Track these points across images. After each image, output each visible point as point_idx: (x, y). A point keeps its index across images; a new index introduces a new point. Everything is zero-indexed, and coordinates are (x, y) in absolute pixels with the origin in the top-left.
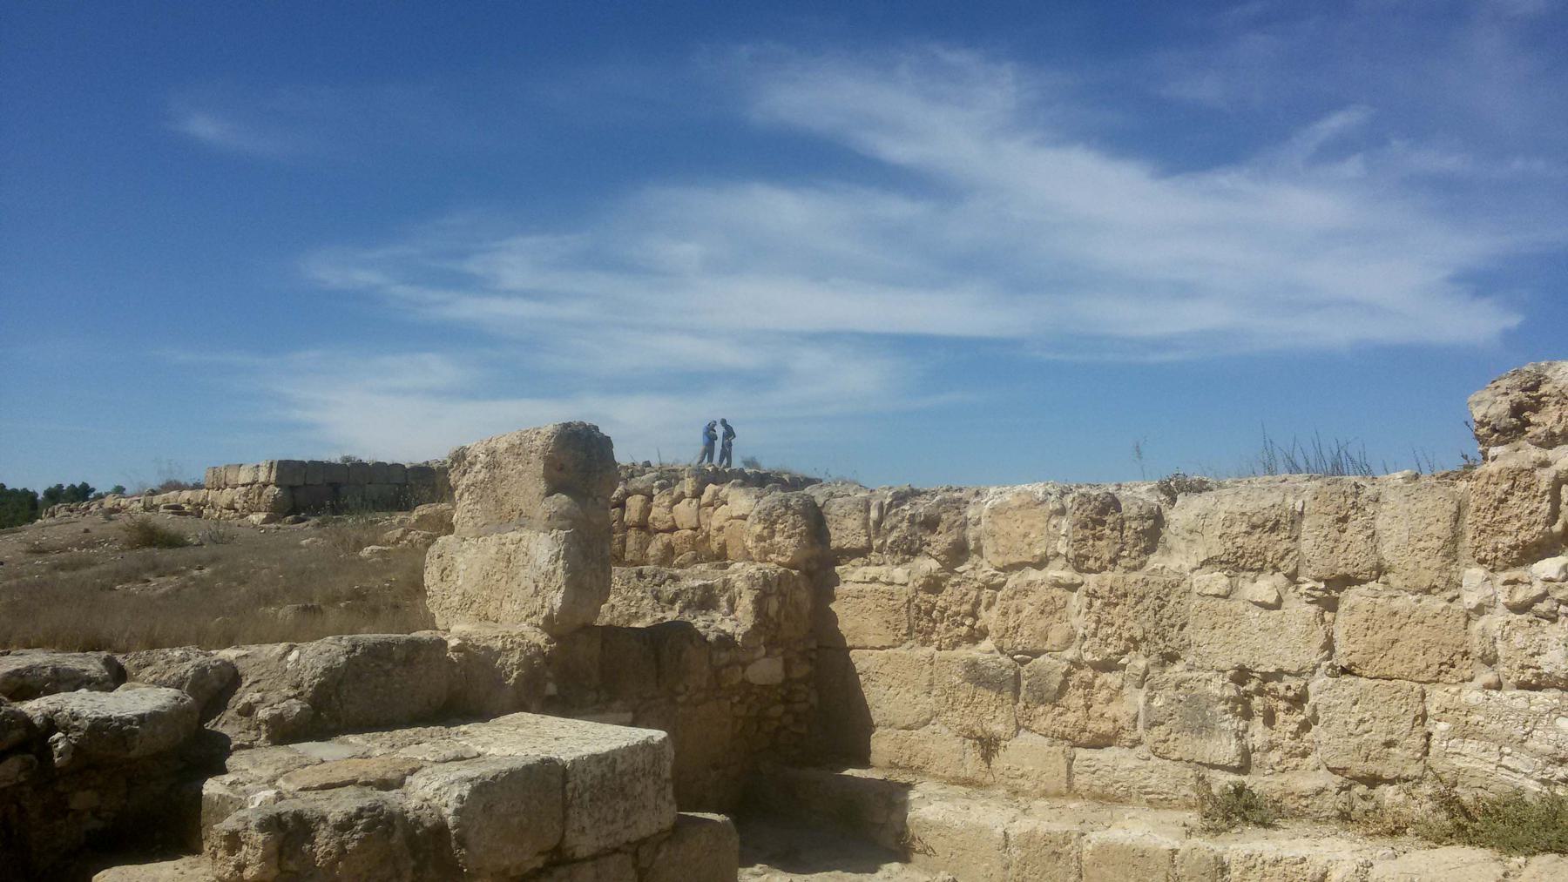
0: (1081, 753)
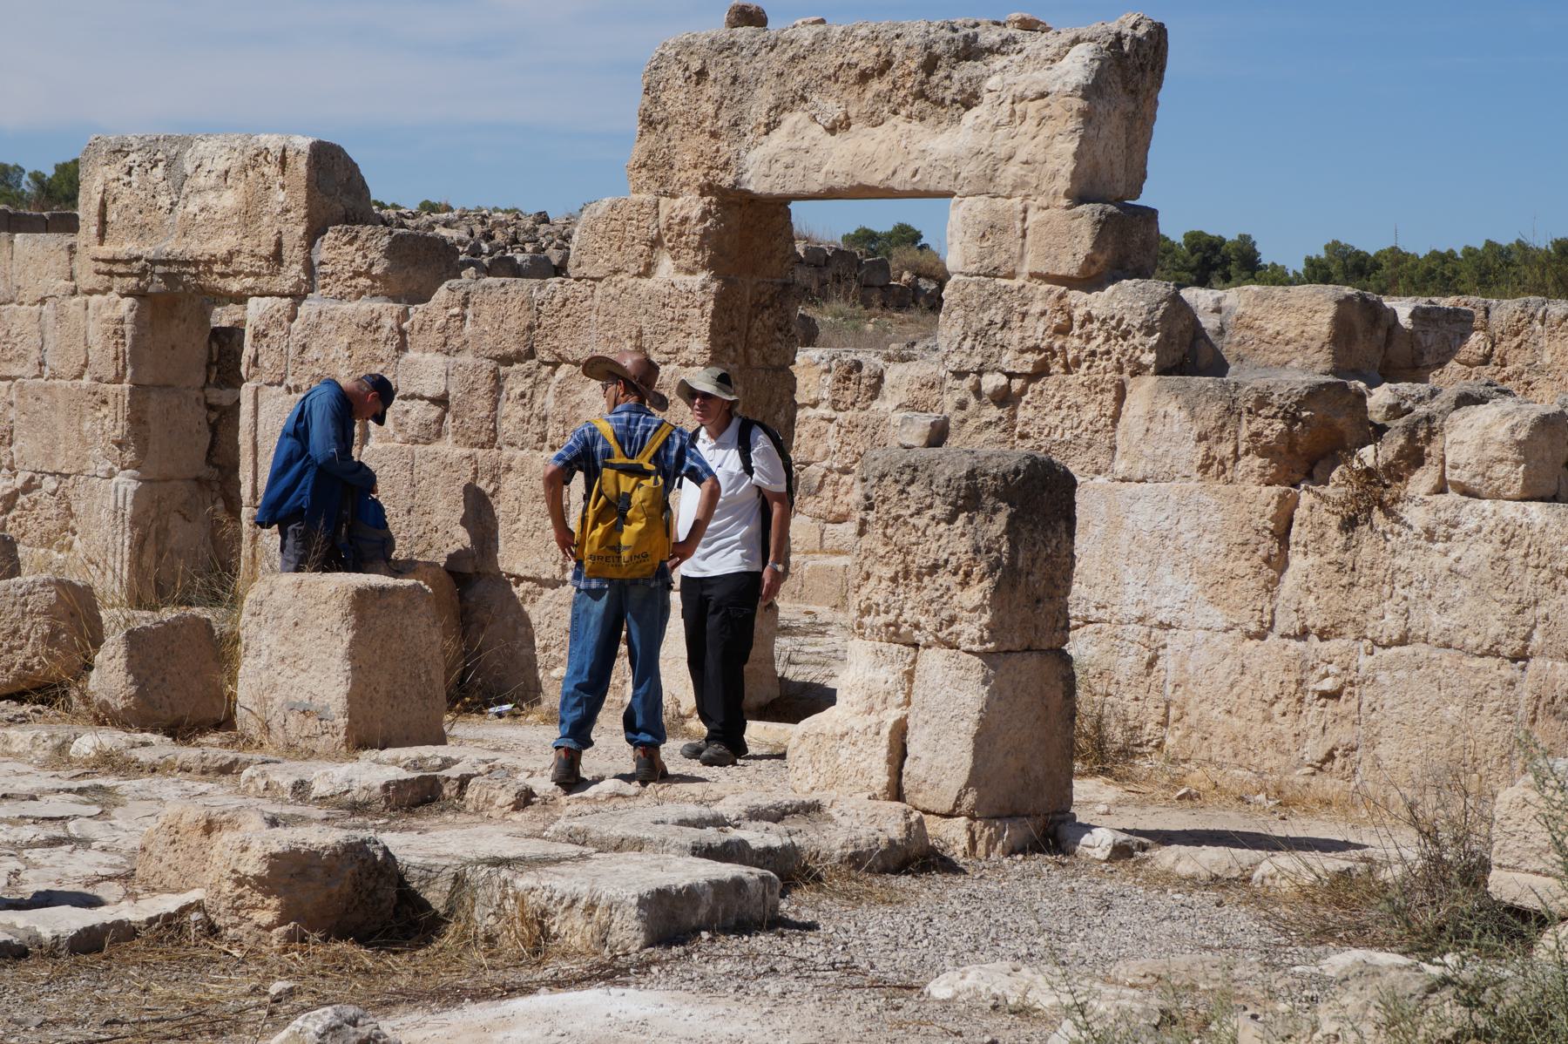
0: (829, 526)
